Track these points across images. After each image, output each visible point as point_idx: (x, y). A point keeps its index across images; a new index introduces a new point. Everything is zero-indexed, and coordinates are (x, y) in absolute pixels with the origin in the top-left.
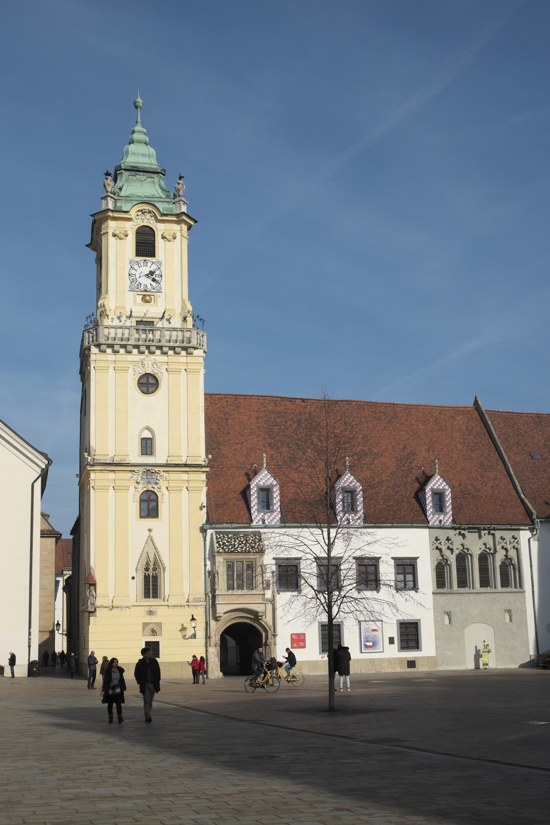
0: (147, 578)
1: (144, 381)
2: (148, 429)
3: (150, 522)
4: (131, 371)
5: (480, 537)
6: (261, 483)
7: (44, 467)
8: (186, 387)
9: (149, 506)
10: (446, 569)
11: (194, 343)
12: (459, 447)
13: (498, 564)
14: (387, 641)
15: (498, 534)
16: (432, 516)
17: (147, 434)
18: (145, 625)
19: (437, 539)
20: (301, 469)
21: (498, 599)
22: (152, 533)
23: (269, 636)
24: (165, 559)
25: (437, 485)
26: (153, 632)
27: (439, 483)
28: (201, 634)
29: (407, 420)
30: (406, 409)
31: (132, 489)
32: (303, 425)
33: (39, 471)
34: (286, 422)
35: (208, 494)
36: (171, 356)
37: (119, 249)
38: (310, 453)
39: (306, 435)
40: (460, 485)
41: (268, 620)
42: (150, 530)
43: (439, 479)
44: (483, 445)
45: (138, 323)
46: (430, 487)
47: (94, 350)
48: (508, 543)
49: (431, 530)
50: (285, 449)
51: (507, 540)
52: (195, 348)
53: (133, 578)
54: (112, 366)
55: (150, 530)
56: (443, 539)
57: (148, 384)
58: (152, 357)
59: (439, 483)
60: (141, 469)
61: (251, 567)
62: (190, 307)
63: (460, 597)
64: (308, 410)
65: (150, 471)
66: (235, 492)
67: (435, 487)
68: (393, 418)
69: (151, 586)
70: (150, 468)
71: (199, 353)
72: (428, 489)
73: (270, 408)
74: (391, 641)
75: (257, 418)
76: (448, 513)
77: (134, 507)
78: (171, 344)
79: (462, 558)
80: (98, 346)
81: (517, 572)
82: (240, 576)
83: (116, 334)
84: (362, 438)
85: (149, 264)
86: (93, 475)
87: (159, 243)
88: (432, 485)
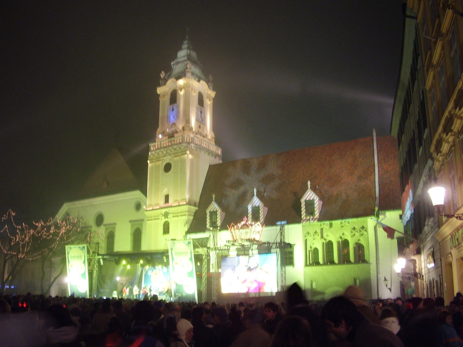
6: (212, 211)
27: (310, 196)
43: (313, 195)
46: (304, 200)
59: (310, 196)
72: (303, 201)
88: (305, 198)
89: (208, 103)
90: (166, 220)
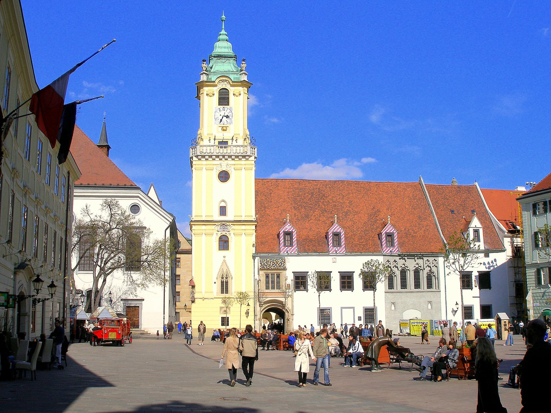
0: (222, 282)
1: (222, 175)
2: (223, 201)
4: (215, 170)
7: (171, 221)
8: (244, 177)
9: (224, 243)
10: (395, 279)
11: (249, 154)
12: (407, 207)
13: (425, 275)
14: (357, 319)
15: (425, 259)
17: (223, 204)
18: (221, 308)
21: (424, 296)
22: (225, 259)
23: (290, 315)
24: (233, 272)
26: (225, 312)
28: (251, 313)
29: (376, 191)
30: (377, 185)
31: (215, 235)
32: (315, 196)
33: (169, 223)
34: (305, 194)
35: (256, 237)
36: (237, 161)
37: (209, 102)
38: (317, 212)
39: (316, 202)
40: (405, 229)
41: (289, 306)
42: (224, 257)
44: (422, 206)
45: (219, 143)
47: (195, 158)
50: (303, 210)
51: (431, 261)
52: (250, 156)
53: (215, 283)
54: (204, 167)
55: (224, 257)
57: (224, 176)
58: (226, 161)
60: (219, 224)
61: (278, 277)
62: (248, 133)
63: (401, 294)
64: (318, 187)
65: (224, 224)
66: (272, 235)
68: (368, 190)
69: (225, 287)
70: (223, 223)
71: (252, 158)
74: (360, 318)
75: (288, 192)
77: (216, 244)
78: (236, 154)
79: (403, 273)
80: (197, 156)
81: (437, 280)
82: (273, 282)
83: (206, 150)
84: (349, 203)
85: (226, 109)
86: (194, 227)
87: (232, 98)
90: (224, 233)
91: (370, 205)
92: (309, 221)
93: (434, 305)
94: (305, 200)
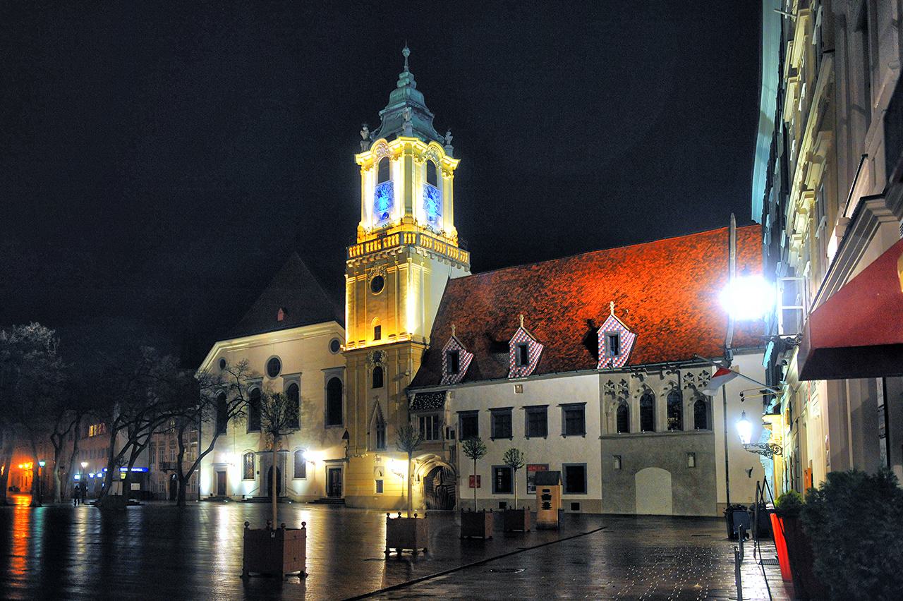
3: (378, 391)
5: (662, 378)
15: (684, 372)
16: (604, 360)
19: (610, 383)
20: (507, 330)
25: (611, 328)
27: (613, 325)
46: (603, 331)
48: (697, 380)
49: (602, 375)
55: (377, 397)
56: (617, 383)
59: (613, 325)
67: (609, 330)
72: (601, 333)
73: (506, 279)
76: (623, 354)
79: (648, 402)
88: (605, 328)
89: (447, 181)
91: (612, 289)
92: (503, 330)
93: (699, 461)
94: (510, 299)
